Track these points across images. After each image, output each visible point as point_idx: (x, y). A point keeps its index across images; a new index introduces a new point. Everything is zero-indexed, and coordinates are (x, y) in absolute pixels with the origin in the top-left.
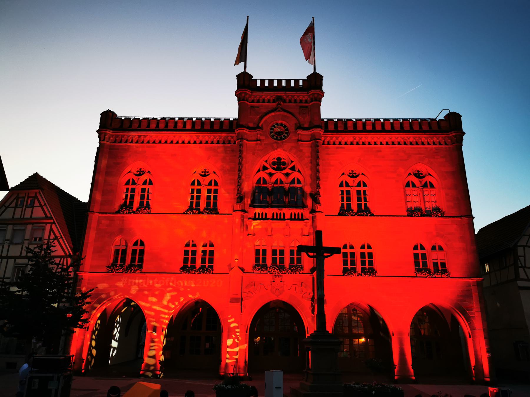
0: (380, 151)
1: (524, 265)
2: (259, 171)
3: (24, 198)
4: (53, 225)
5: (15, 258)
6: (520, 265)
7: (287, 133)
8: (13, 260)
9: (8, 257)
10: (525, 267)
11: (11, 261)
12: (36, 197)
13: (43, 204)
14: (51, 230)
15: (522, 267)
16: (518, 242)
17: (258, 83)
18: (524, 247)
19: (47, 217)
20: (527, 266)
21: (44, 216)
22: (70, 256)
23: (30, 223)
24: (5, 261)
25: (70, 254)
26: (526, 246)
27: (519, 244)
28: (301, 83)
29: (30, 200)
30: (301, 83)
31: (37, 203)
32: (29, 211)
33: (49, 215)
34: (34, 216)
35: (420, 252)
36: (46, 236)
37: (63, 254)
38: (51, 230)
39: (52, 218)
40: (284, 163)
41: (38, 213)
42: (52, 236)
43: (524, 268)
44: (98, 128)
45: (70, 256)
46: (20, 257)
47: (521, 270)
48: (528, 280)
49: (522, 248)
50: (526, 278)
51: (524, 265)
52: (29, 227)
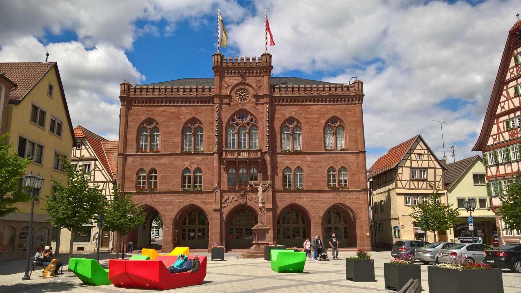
28: (257, 59)
30: (257, 59)
33: (93, 156)
38: (95, 164)
41: (86, 154)
47: (399, 182)
48: (403, 188)
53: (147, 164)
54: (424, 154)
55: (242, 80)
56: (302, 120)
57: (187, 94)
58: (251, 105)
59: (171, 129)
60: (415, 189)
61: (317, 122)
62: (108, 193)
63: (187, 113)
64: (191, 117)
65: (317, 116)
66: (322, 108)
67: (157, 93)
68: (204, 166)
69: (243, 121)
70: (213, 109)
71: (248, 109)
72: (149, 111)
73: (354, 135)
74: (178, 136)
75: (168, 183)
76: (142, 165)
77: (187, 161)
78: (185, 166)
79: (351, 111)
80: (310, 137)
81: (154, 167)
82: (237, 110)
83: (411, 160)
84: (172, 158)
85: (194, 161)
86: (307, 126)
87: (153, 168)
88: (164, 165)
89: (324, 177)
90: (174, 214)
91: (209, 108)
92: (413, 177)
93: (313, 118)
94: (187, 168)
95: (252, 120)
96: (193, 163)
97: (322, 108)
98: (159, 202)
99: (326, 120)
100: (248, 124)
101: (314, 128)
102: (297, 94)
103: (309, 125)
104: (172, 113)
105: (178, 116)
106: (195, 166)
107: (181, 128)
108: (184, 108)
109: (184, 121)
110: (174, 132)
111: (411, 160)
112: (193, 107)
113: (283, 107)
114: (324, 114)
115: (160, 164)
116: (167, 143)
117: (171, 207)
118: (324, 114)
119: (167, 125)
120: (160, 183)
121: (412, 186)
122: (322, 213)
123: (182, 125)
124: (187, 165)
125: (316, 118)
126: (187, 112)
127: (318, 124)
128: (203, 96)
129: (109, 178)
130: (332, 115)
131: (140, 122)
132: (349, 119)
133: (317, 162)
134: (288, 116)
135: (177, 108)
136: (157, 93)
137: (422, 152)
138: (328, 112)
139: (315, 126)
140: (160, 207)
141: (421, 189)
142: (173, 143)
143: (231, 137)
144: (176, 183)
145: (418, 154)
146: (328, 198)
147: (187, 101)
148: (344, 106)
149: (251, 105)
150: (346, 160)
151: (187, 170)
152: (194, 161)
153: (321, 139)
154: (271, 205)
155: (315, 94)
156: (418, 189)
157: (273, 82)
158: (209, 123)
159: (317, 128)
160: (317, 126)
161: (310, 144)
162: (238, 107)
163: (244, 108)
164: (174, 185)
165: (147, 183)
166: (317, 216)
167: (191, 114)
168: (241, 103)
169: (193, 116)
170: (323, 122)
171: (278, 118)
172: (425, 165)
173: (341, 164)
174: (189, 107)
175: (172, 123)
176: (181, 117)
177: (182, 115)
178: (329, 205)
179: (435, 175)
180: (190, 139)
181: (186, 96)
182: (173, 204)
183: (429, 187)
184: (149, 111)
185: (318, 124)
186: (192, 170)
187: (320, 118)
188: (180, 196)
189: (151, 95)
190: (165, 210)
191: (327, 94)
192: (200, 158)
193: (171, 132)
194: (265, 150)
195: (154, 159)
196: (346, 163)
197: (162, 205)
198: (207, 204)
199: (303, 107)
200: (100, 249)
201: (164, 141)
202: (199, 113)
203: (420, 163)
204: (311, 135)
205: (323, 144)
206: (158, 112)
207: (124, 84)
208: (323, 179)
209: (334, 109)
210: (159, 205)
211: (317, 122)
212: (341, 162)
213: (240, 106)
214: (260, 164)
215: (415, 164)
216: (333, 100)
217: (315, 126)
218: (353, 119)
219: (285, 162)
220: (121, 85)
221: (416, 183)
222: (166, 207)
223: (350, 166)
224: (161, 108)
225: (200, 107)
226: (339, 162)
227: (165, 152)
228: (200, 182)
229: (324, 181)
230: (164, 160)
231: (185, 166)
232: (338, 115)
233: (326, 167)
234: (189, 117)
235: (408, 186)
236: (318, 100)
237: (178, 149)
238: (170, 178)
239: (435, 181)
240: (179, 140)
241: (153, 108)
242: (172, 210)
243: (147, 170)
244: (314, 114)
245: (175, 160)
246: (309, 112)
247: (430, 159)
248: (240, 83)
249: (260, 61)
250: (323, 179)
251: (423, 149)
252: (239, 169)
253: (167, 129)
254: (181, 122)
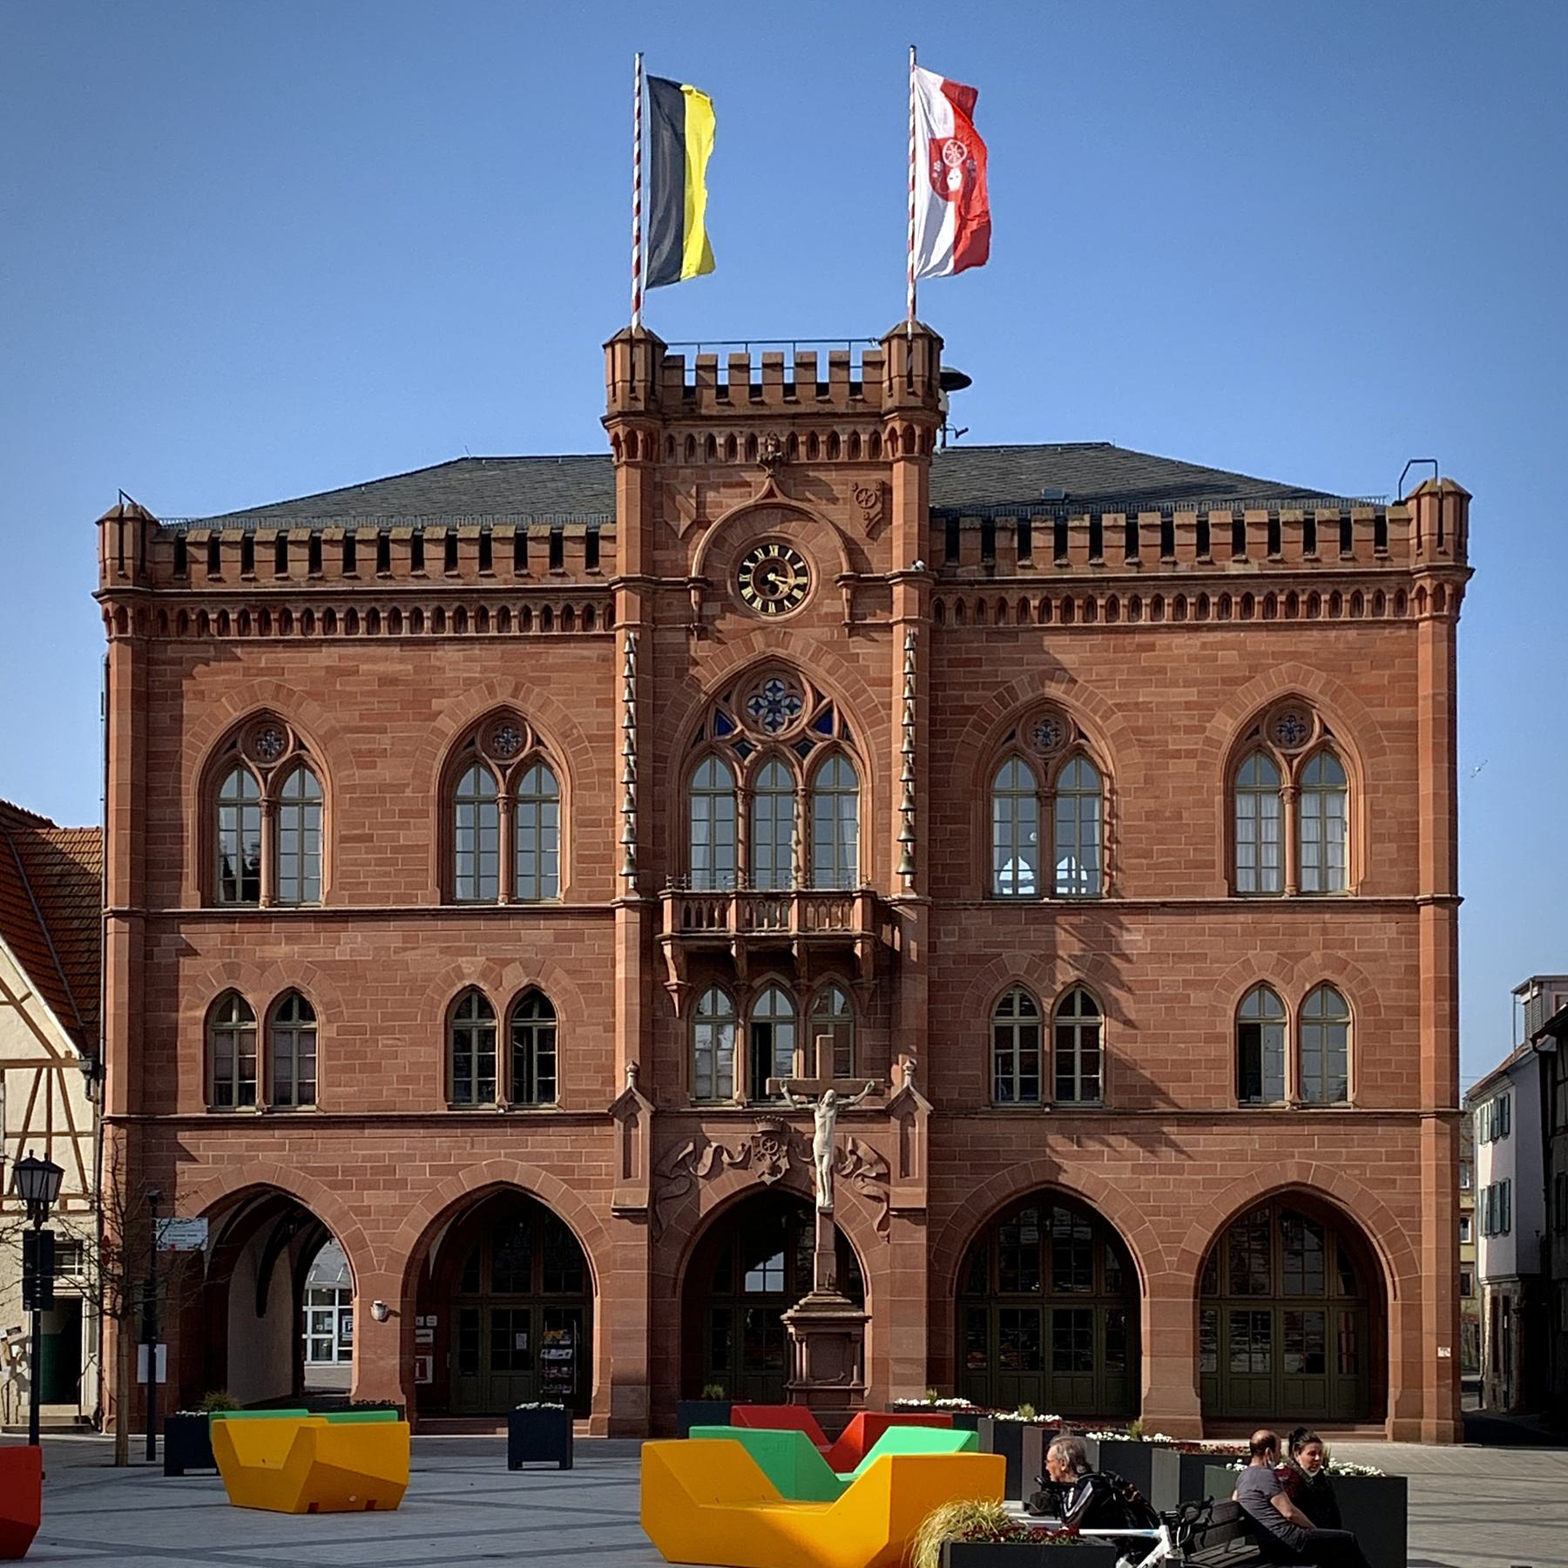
0: (1151, 647)
17: (690, 364)
22: (68, 1061)
25: (69, 1053)
45: (68, 1061)
53: (263, 966)
55: (771, 493)
56: (1105, 718)
57: (470, 576)
58: (823, 633)
59: (385, 772)
61: (1189, 730)
62: (59, 1124)
63: (469, 682)
64: (492, 704)
65: (1192, 695)
66: (1222, 646)
67: (298, 564)
68: (566, 981)
69: (774, 725)
70: (609, 660)
71: (802, 661)
72: (261, 672)
73: (1402, 802)
74: (423, 814)
75: (375, 1068)
76: (232, 970)
77: (472, 952)
78: (461, 977)
79: (1390, 666)
80: (1151, 815)
81: (297, 982)
82: (740, 664)
84: (391, 933)
85: (508, 950)
86: (1135, 751)
87: (293, 992)
88: (350, 971)
89: (1220, 1038)
90: (407, 1235)
91: (592, 651)
93: (1169, 706)
94: (474, 988)
95: (822, 722)
96: (505, 963)
97: (1222, 646)
98: (334, 1171)
99: (1245, 715)
100: (803, 746)
101: (1175, 766)
102: (1081, 569)
103: (1143, 744)
104: (387, 681)
105: (419, 702)
106: (514, 980)
107: (437, 767)
108: (449, 655)
109: (451, 727)
110: (401, 788)
112: (499, 648)
113: (1003, 648)
114: (1224, 681)
115: (330, 968)
116: (361, 853)
117: (392, 1198)
118: (1234, 681)
119: (358, 754)
120: (330, 1070)
122: (1198, 1239)
123: (443, 752)
124: (471, 970)
125: (1188, 705)
126: (465, 678)
127: (1194, 742)
128: (557, 583)
129: (63, 1043)
130: (1278, 691)
131: (212, 740)
132: (1378, 714)
133: (1180, 957)
134: (1026, 696)
135: (410, 652)
136: (298, 564)
138: (1254, 669)
139: (1177, 755)
140: (337, 1195)
142: (395, 850)
143: (709, 827)
144: (416, 1067)
146: (1240, 1155)
147: (467, 612)
148: (1352, 634)
149: (823, 633)
150: (1344, 944)
151: (470, 1002)
152: (508, 950)
153: (1211, 828)
154: (922, 1190)
155: (1183, 569)
157: (954, 492)
158: (590, 739)
159: (1192, 765)
160: (1191, 754)
161: (1147, 854)
162: (751, 648)
163: (781, 652)
164: (404, 1079)
165: (264, 1061)
166: (1170, 1252)
167: (491, 689)
168: (763, 628)
169: (502, 698)
170: (1226, 727)
171: (970, 710)
173: (1314, 967)
174: (476, 650)
175: (385, 742)
176: (436, 704)
177: (441, 694)
178: (1241, 1196)
180: (482, 828)
181: (457, 585)
182: (403, 1183)
184: (261, 672)
185: (1194, 742)
186: (500, 1002)
187: (1205, 709)
188: (441, 1140)
189: (268, 581)
190: (363, 1211)
191: (1253, 569)
192: (543, 932)
193: (384, 788)
194: (898, 887)
195: (290, 939)
196: (1343, 966)
197: (347, 1185)
198: (584, 1184)
199: (1113, 640)
200: (44, 1410)
201: (344, 839)
202: (536, 681)
204: (1151, 804)
205: (1219, 857)
206: (305, 679)
207: (120, 520)
208: (1213, 1051)
209: (1294, 655)
210: (334, 1186)
211: (1189, 730)
212: (1317, 956)
213: (758, 640)
214: (867, 970)
216: (1287, 600)
217: (1177, 755)
218: (1400, 713)
219: (1006, 954)
220: (101, 522)
222: (369, 1198)
223: (1365, 983)
224: (327, 657)
225: (541, 648)
226: (1317, 947)
227: (352, 900)
228: (547, 1065)
229: (1216, 1064)
230: (353, 943)
231: (461, 977)
232: (1312, 688)
233: (1230, 988)
234: (478, 706)
236: (1197, 601)
237: (424, 886)
238: (383, 1040)
240: (426, 832)
241: (283, 655)
242: (400, 1212)
243: (259, 1000)
244: (1174, 684)
245: (410, 942)
246: (1144, 671)
248: (757, 507)
249: (873, 374)
250: (1213, 1051)
252: (753, 994)
253: (359, 776)
254: (435, 731)
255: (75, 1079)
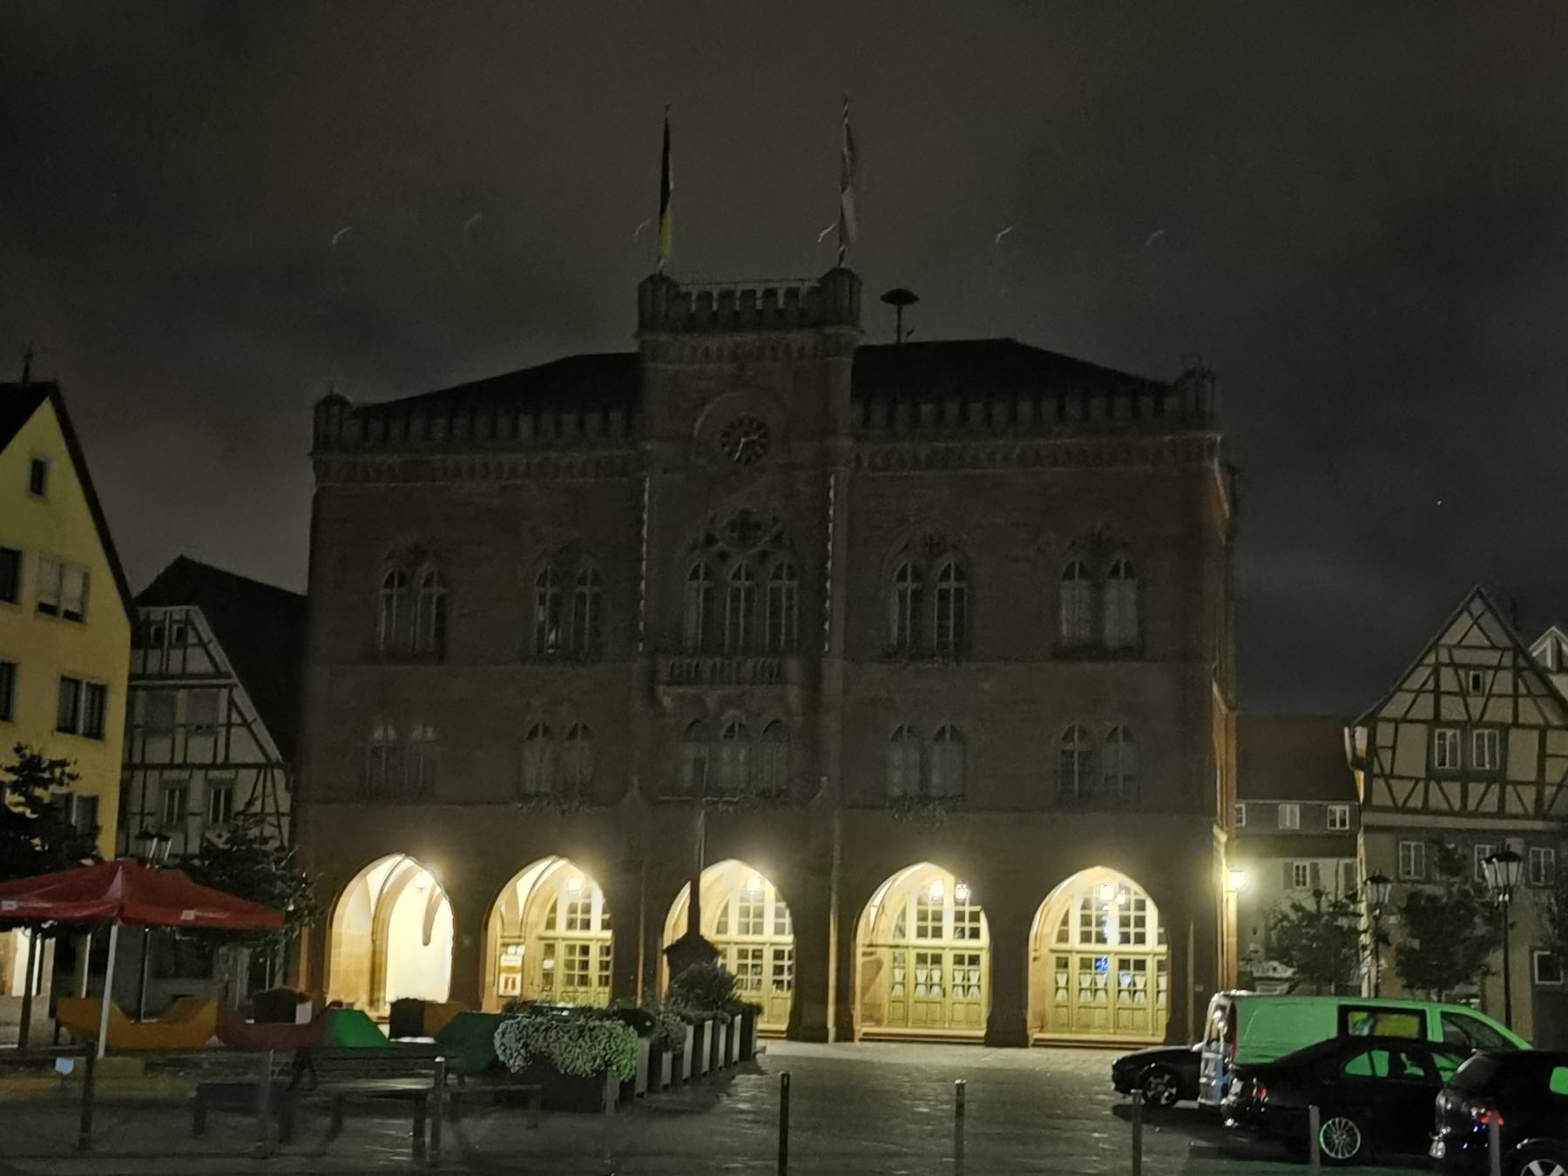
1: (1387, 770)
2: (693, 548)
3: (163, 621)
4: (235, 692)
5: (161, 767)
6: (1376, 769)
7: (762, 446)
8: (157, 773)
9: (146, 767)
10: (1392, 775)
11: (153, 776)
12: (188, 621)
13: (205, 639)
14: (232, 703)
15: (1382, 775)
16: (1380, 708)
18: (1397, 722)
19: (218, 674)
20: (1396, 772)
21: (211, 669)
23: (184, 687)
24: (139, 774)
26: (1405, 720)
27: (1385, 713)
29: (175, 627)
31: (192, 639)
32: (176, 655)
33: (223, 669)
34: (191, 668)
35: (1075, 746)
36: (222, 719)
37: (262, 760)
38: (232, 703)
39: (229, 676)
40: (757, 526)
41: (198, 662)
42: (235, 718)
43: (1389, 777)
44: (310, 449)
45: (279, 766)
46: (171, 766)
49: (1392, 726)
50: (1390, 803)
51: (1387, 770)
52: (182, 695)
54: (1497, 668)
60: (1451, 813)
62: (270, 808)
83: (1438, 693)
92: (1442, 763)
111: (1438, 693)
121: (1436, 799)
129: (274, 753)
137: (1493, 658)
141: (1474, 815)
145: (1468, 667)
156: (1464, 812)
172: (1500, 711)
179: (1543, 755)
183: (1513, 807)
203: (1476, 703)
215: (1452, 709)
221: (1453, 789)
235: (1416, 802)
239: (1540, 783)
247: (1522, 690)
251: (1494, 647)
255: (279, 774)
